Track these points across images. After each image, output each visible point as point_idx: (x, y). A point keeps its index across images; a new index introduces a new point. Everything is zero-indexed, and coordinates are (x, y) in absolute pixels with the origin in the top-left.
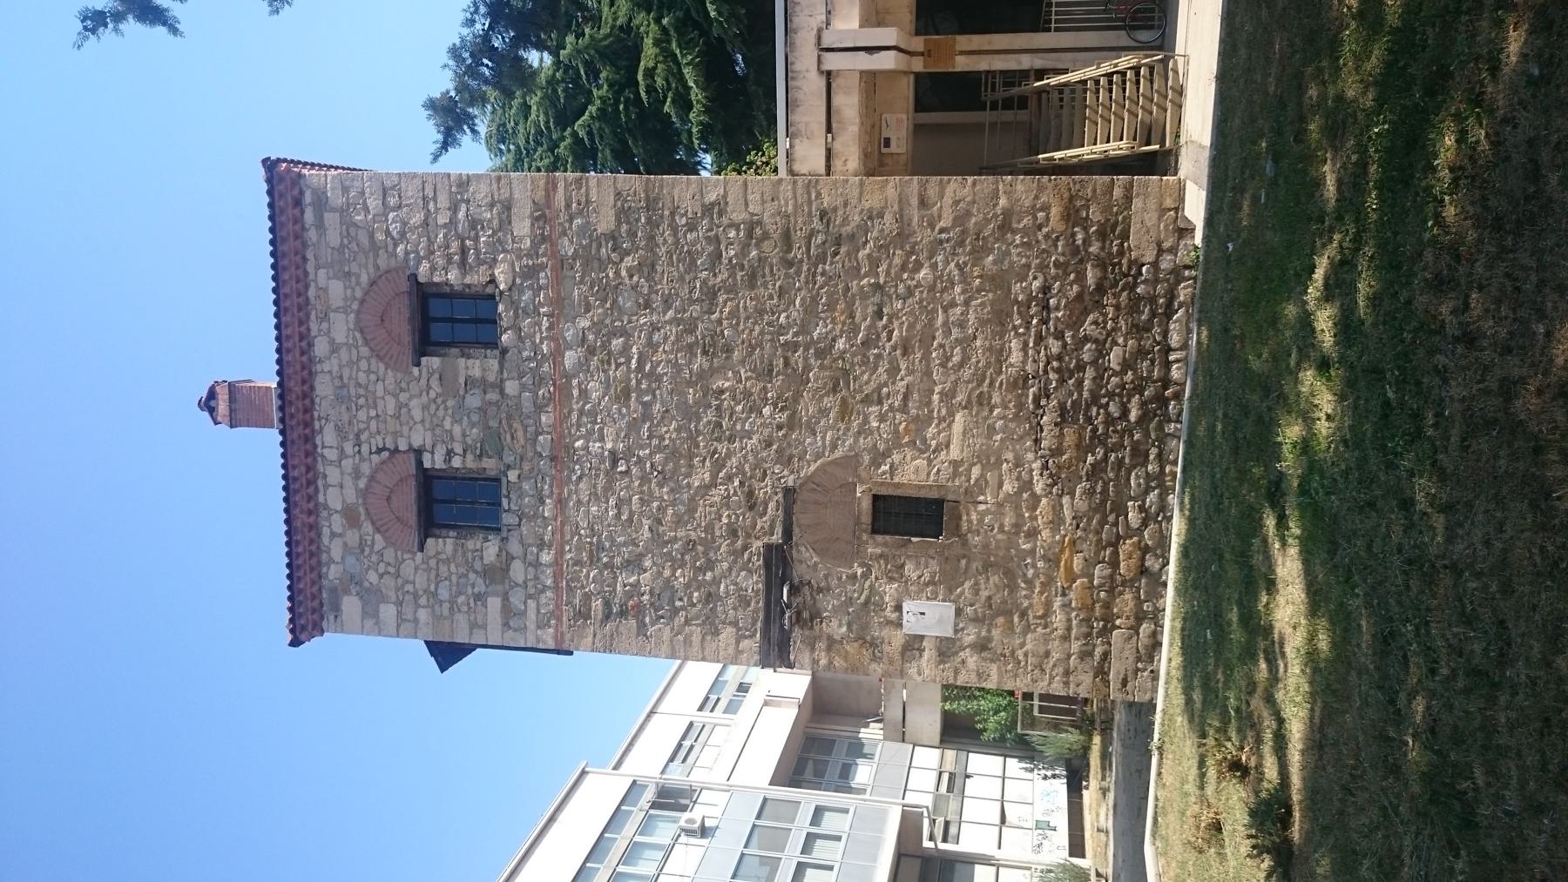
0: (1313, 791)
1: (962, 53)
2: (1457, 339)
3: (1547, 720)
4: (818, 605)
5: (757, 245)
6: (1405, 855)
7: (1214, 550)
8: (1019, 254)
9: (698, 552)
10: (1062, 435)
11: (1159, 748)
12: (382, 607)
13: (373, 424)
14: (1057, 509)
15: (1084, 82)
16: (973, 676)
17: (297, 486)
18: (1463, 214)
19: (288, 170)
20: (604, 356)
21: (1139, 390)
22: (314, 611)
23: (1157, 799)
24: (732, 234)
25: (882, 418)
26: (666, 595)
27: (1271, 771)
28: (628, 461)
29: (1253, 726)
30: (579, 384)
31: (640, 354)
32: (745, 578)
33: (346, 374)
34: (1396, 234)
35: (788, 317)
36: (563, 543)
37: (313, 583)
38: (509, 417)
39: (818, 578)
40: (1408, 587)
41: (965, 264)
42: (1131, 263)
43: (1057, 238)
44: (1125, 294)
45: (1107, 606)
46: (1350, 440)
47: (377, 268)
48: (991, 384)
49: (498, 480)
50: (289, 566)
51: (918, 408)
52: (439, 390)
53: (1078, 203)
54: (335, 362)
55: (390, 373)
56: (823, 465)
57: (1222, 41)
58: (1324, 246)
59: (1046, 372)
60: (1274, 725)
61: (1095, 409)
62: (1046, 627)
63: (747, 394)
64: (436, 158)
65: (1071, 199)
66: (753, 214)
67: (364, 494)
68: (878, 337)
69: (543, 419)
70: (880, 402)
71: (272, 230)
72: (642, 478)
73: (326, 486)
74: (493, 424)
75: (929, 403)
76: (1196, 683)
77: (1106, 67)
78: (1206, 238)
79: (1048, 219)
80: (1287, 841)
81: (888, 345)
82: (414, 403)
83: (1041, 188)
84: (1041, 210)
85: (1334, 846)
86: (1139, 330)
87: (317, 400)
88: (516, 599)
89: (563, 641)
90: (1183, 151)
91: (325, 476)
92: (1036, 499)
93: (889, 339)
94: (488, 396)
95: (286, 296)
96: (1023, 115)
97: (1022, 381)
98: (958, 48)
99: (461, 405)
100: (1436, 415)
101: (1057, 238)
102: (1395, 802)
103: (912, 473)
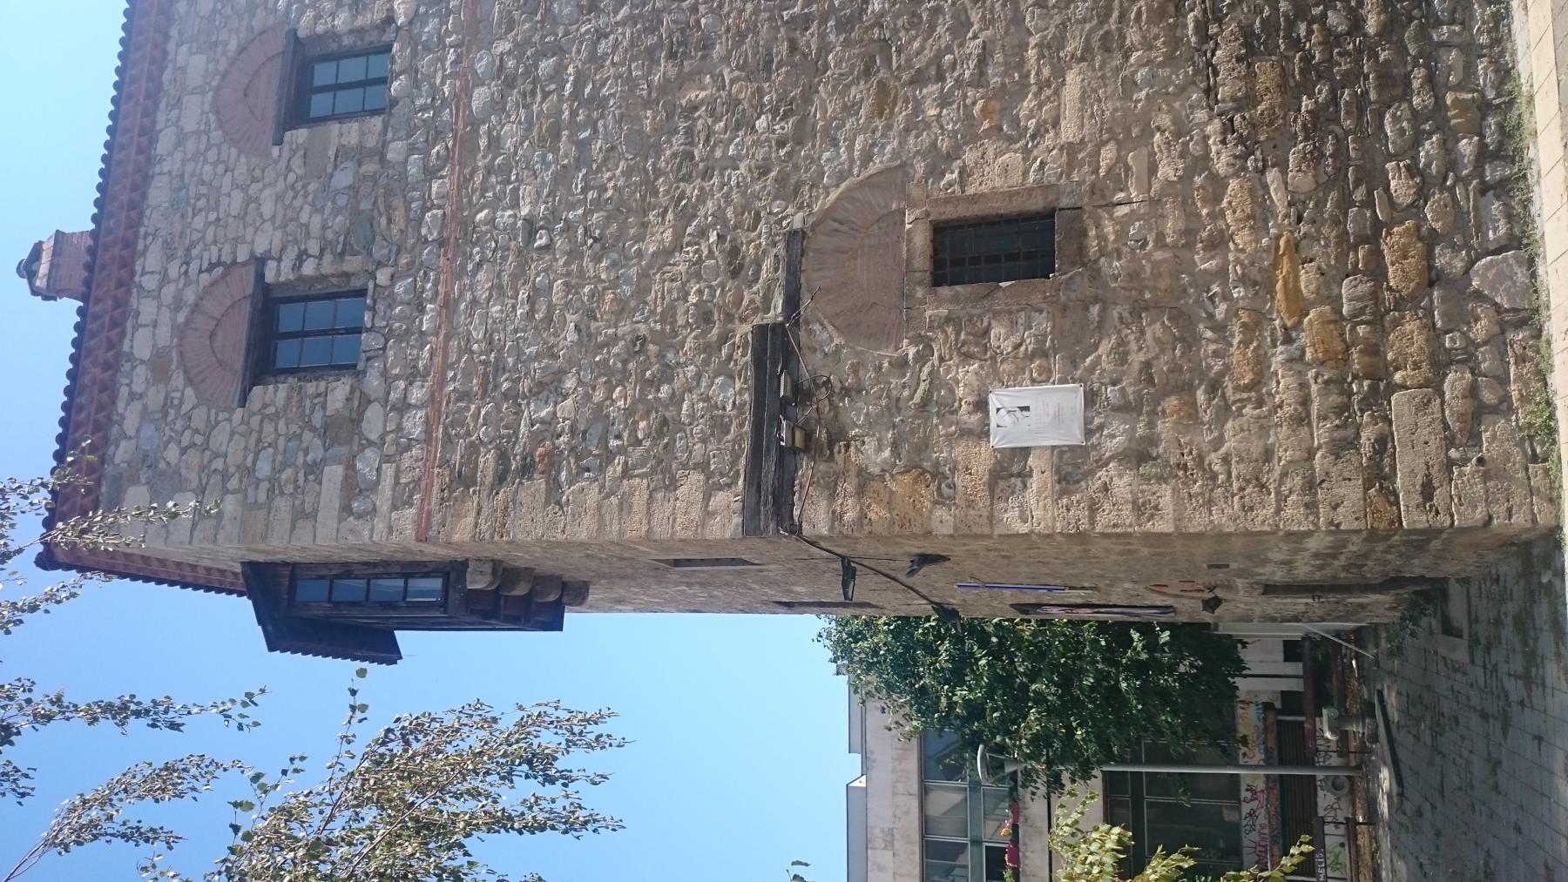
4: (842, 418)
10: (1251, 76)
14: (1258, 193)
26: (596, 430)
28: (550, 231)
31: (578, 73)
32: (723, 388)
38: (389, 193)
45: (1374, 350)
47: (251, 29)
48: (1123, 17)
49: (362, 293)
51: (1005, 74)
54: (178, 156)
55: (243, 159)
56: (848, 190)
63: (732, 103)
67: (180, 331)
74: (365, 205)
82: (267, 192)
87: (148, 212)
88: (367, 465)
89: (429, 526)
91: (138, 313)
92: (1217, 185)
94: (364, 169)
95: (134, 80)
103: (997, 175)
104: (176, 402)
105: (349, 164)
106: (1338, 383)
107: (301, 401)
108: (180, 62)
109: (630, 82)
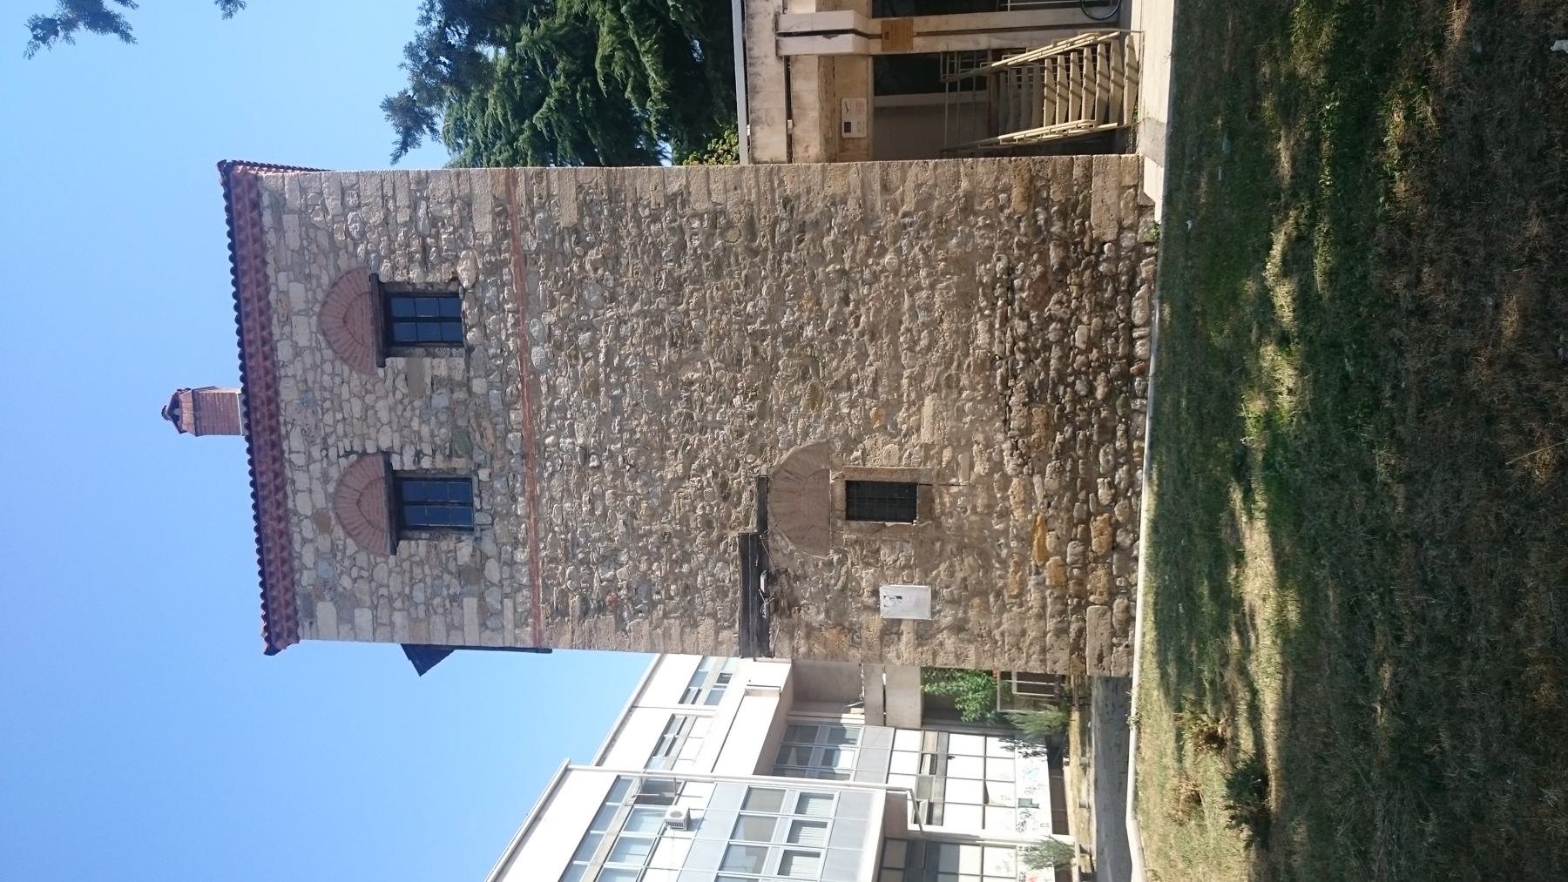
0: (1288, 760)
1: (919, 34)
2: (1410, 313)
3: (1507, 683)
4: (796, 593)
5: (722, 235)
6: (1378, 821)
7: (1183, 525)
8: (982, 236)
9: (674, 545)
11: (1137, 723)
12: (357, 612)
13: (340, 427)
14: (1028, 488)
15: (1042, 61)
16: (951, 657)
17: (265, 493)
18: (1413, 190)
19: (245, 173)
20: (571, 351)
21: (1104, 367)
22: (289, 618)
23: (1136, 773)
24: (696, 224)
25: (852, 404)
26: (643, 589)
27: (1247, 742)
28: (599, 457)
29: (1227, 698)
30: (548, 380)
31: (608, 349)
32: (722, 569)
33: (310, 377)
34: (1349, 210)
35: (754, 306)
36: (537, 540)
37: (287, 590)
39: (794, 566)
40: (1372, 557)
41: (930, 247)
42: (1092, 241)
43: (1019, 219)
44: (1088, 272)
45: (1081, 583)
46: (1312, 414)
48: (959, 366)
49: (468, 480)
50: (261, 573)
51: (888, 393)
52: (405, 391)
53: (1039, 184)
54: (298, 365)
56: (795, 453)
57: (1176, 18)
58: (1281, 222)
59: (1012, 352)
60: (1248, 697)
61: (1061, 388)
62: (1021, 606)
63: (717, 385)
64: (396, 158)
65: (1032, 180)
66: (716, 204)
67: (334, 498)
68: (846, 323)
69: (512, 416)
70: (850, 388)
71: (230, 234)
72: (614, 473)
73: (295, 492)
74: (461, 423)
75: (899, 387)
76: (1170, 656)
77: (1063, 46)
78: (1165, 216)
79: (1009, 200)
80: (1264, 810)
81: (856, 332)
82: (380, 404)
83: (1002, 170)
84: (1003, 191)
85: (1309, 814)
86: (1102, 308)
88: (492, 599)
89: (541, 639)
90: (1141, 128)
91: (294, 482)
92: (1007, 480)
93: (857, 325)
94: (456, 396)
95: (247, 300)
96: (981, 96)
97: (989, 362)
98: (916, 29)
99: (428, 406)
100: (1393, 388)
101: (1019, 219)
102: (1367, 768)
103: (884, 458)
106: (1061, 599)
108: (282, 284)
109: (644, 358)
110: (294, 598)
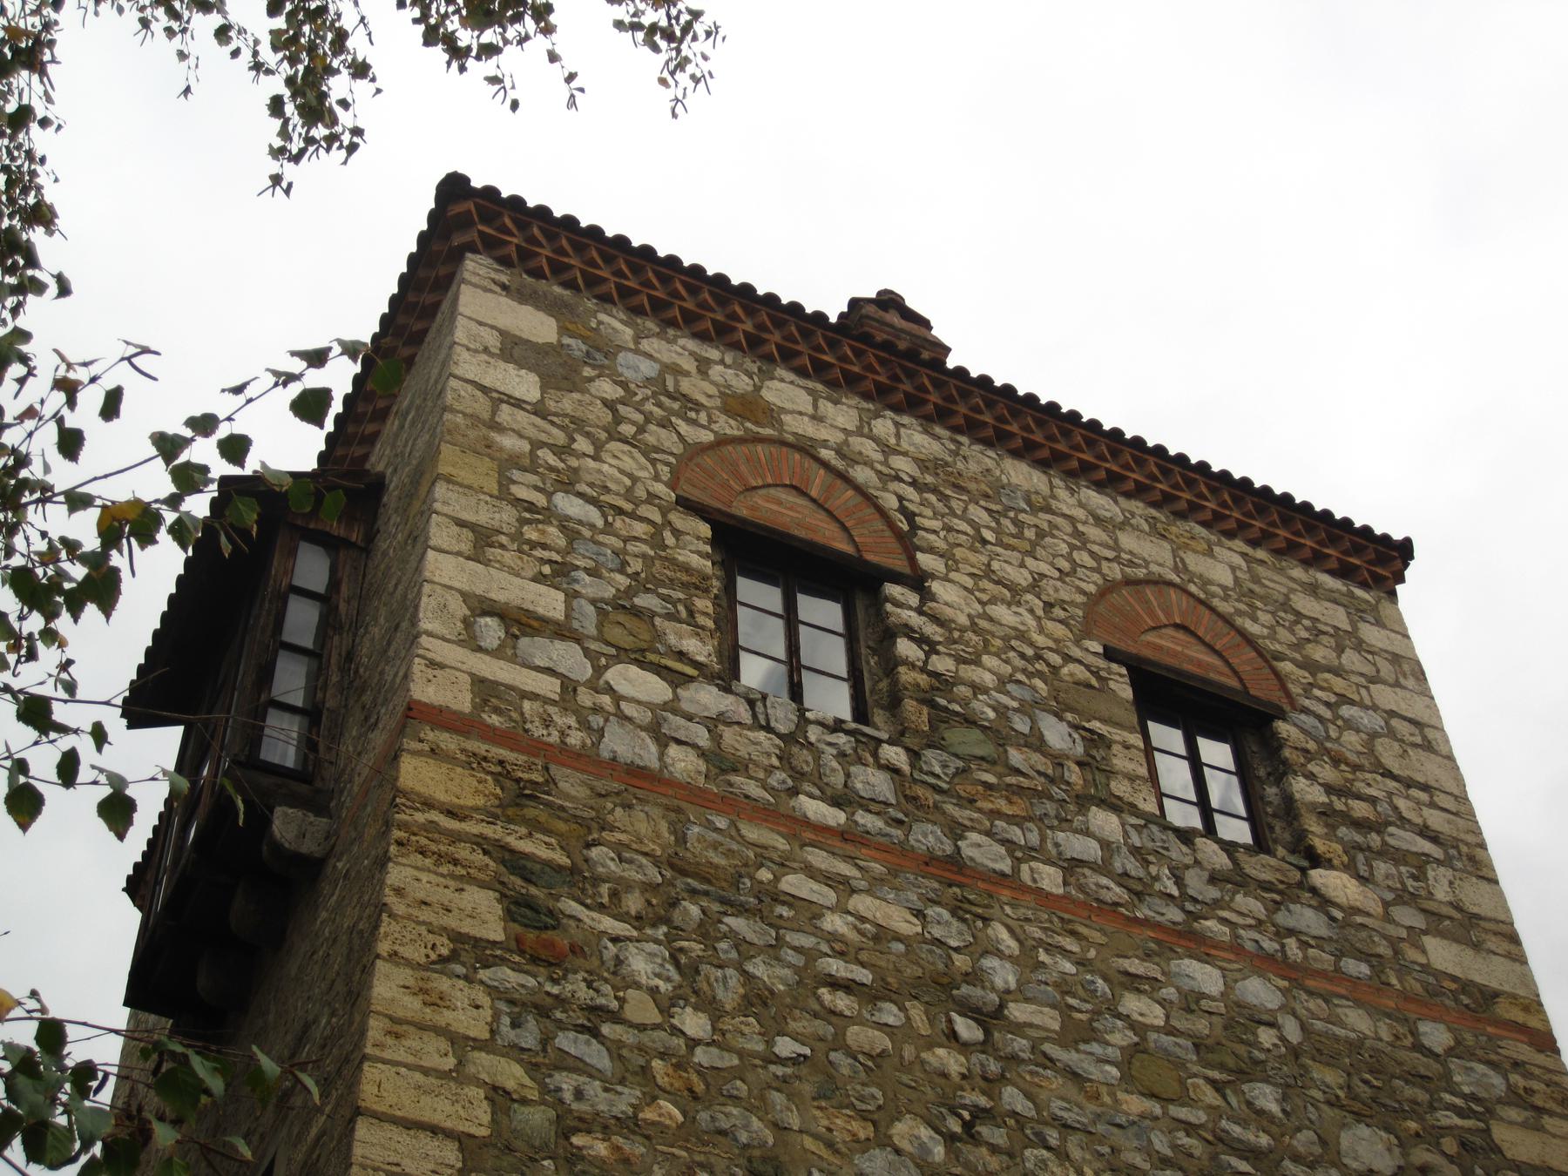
12: (533, 378)
54: (1080, 513)
67: (806, 448)
73: (810, 392)
87: (991, 453)
91: (836, 402)
104: (693, 415)
105: (1080, 749)
107: (685, 586)
110: (570, 285)
